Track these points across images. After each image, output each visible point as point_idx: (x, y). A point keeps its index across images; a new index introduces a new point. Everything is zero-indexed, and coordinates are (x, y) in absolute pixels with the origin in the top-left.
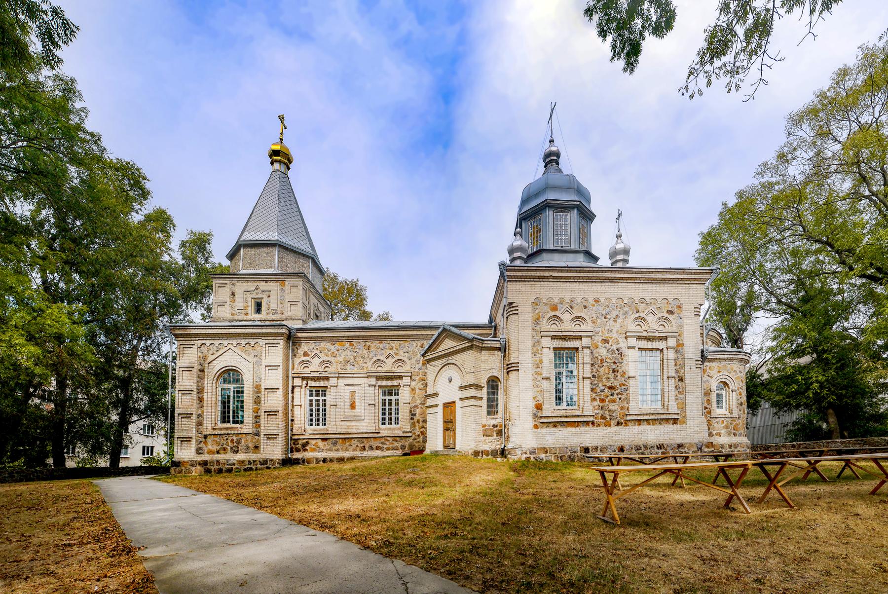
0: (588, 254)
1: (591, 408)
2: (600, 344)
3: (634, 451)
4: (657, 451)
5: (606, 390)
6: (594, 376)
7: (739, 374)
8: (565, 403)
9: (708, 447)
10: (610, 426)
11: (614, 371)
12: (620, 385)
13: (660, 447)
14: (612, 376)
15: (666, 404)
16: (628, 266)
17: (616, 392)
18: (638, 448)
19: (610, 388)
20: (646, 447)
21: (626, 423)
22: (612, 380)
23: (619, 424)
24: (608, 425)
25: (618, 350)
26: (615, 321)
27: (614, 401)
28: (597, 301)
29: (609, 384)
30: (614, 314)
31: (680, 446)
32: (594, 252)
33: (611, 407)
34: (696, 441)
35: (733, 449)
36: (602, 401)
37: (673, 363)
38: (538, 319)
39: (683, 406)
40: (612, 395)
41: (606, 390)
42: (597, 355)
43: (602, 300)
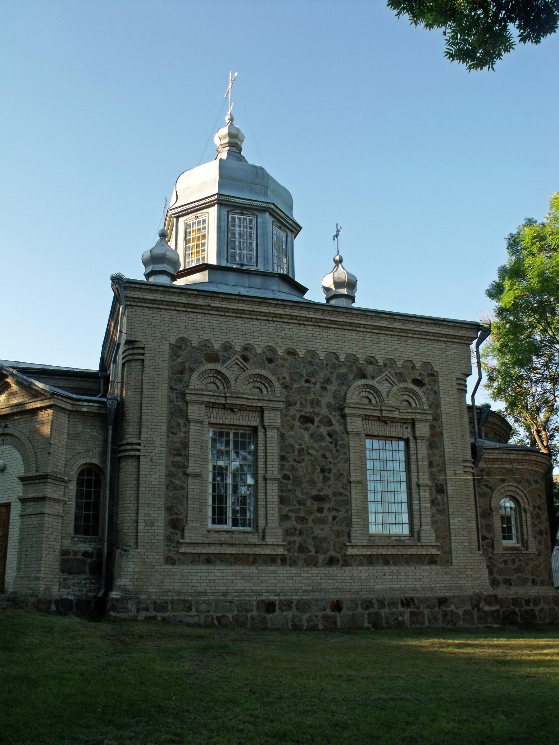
0: (288, 280)
1: (280, 532)
2: (297, 423)
3: (360, 610)
4: (400, 609)
5: (309, 503)
6: (286, 477)
7: (534, 486)
8: (230, 521)
9: (490, 604)
10: (315, 565)
11: (323, 470)
12: (334, 494)
13: (408, 602)
14: (318, 477)
15: (416, 529)
16: (354, 305)
17: (326, 506)
18: (368, 604)
19: (317, 498)
20: (381, 603)
21: (347, 561)
22: (319, 485)
23: (332, 561)
24: (312, 562)
25: (330, 435)
26: (324, 388)
27: (323, 521)
28: (292, 353)
29: (315, 492)
30: (321, 376)
31: (442, 601)
32: (298, 279)
33: (318, 531)
34: (470, 593)
35: (532, 607)
36: (302, 520)
37: (426, 463)
38: (182, 372)
39: (444, 534)
40: (320, 510)
41: (309, 503)
42: (292, 441)
43: (301, 353)
